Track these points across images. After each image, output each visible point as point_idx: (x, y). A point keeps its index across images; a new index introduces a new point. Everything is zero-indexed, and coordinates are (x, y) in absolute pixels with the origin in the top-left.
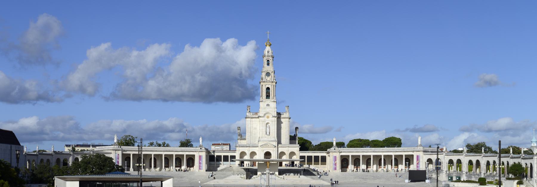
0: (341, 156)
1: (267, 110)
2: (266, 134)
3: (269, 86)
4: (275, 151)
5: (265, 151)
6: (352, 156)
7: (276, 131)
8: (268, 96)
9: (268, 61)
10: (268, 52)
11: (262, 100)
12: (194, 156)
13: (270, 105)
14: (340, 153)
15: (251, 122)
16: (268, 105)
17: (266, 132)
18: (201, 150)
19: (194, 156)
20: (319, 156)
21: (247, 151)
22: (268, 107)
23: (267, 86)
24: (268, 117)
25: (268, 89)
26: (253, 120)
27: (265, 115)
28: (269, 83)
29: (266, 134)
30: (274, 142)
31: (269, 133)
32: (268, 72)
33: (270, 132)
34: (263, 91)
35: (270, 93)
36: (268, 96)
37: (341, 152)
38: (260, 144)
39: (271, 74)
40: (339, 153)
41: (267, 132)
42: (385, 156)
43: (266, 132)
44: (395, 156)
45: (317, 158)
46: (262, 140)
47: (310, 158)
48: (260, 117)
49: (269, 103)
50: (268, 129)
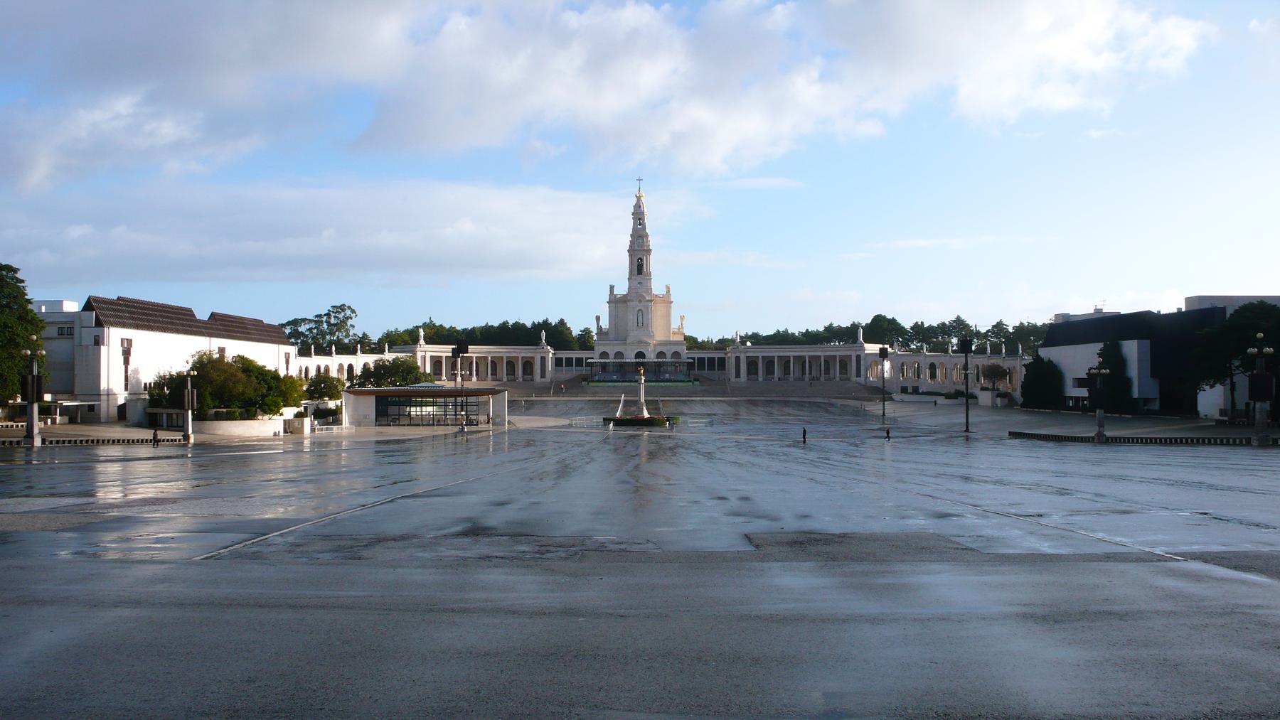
0: (747, 357)
5: (636, 352)
12: (533, 358)
19: (533, 358)
24: (640, 301)
37: (747, 352)
42: (809, 357)
44: (824, 356)
45: (711, 360)
47: (701, 360)
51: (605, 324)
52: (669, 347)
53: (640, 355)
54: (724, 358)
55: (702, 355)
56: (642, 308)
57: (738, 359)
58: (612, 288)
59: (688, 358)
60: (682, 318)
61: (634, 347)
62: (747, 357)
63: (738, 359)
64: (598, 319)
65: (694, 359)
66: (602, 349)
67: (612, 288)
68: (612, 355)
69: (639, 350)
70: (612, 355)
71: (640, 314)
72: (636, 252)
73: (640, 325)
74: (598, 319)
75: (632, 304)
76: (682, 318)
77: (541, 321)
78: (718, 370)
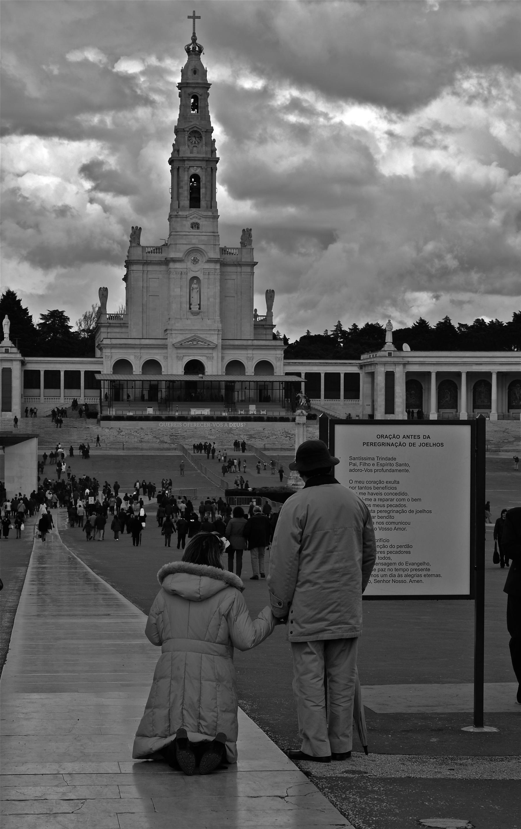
0: (408, 374)
1: (194, 241)
2: (190, 309)
3: (198, 171)
4: (215, 358)
5: (186, 360)
6: (469, 374)
7: (218, 300)
14: (405, 364)
15: (145, 276)
16: (195, 226)
17: (190, 304)
20: (339, 374)
23: (193, 171)
24: (195, 261)
26: (150, 268)
27: (189, 253)
28: (198, 163)
29: (190, 309)
30: (213, 332)
31: (198, 307)
32: (195, 129)
33: (199, 305)
34: (182, 184)
35: (202, 191)
37: (408, 363)
38: (175, 338)
39: (204, 138)
40: (401, 367)
41: (193, 304)
43: (190, 304)
46: (178, 325)
48: (174, 260)
49: (198, 221)
50: (195, 295)
54: (358, 374)
55: (315, 369)
56: (201, 277)
57: (390, 377)
59: (287, 374)
61: (184, 351)
62: (408, 374)
63: (390, 377)
65: (299, 374)
66: (119, 355)
68: (137, 369)
69: (192, 358)
70: (137, 369)
71: (194, 286)
72: (187, 164)
73: (195, 308)
75: (178, 265)
78: (345, 398)
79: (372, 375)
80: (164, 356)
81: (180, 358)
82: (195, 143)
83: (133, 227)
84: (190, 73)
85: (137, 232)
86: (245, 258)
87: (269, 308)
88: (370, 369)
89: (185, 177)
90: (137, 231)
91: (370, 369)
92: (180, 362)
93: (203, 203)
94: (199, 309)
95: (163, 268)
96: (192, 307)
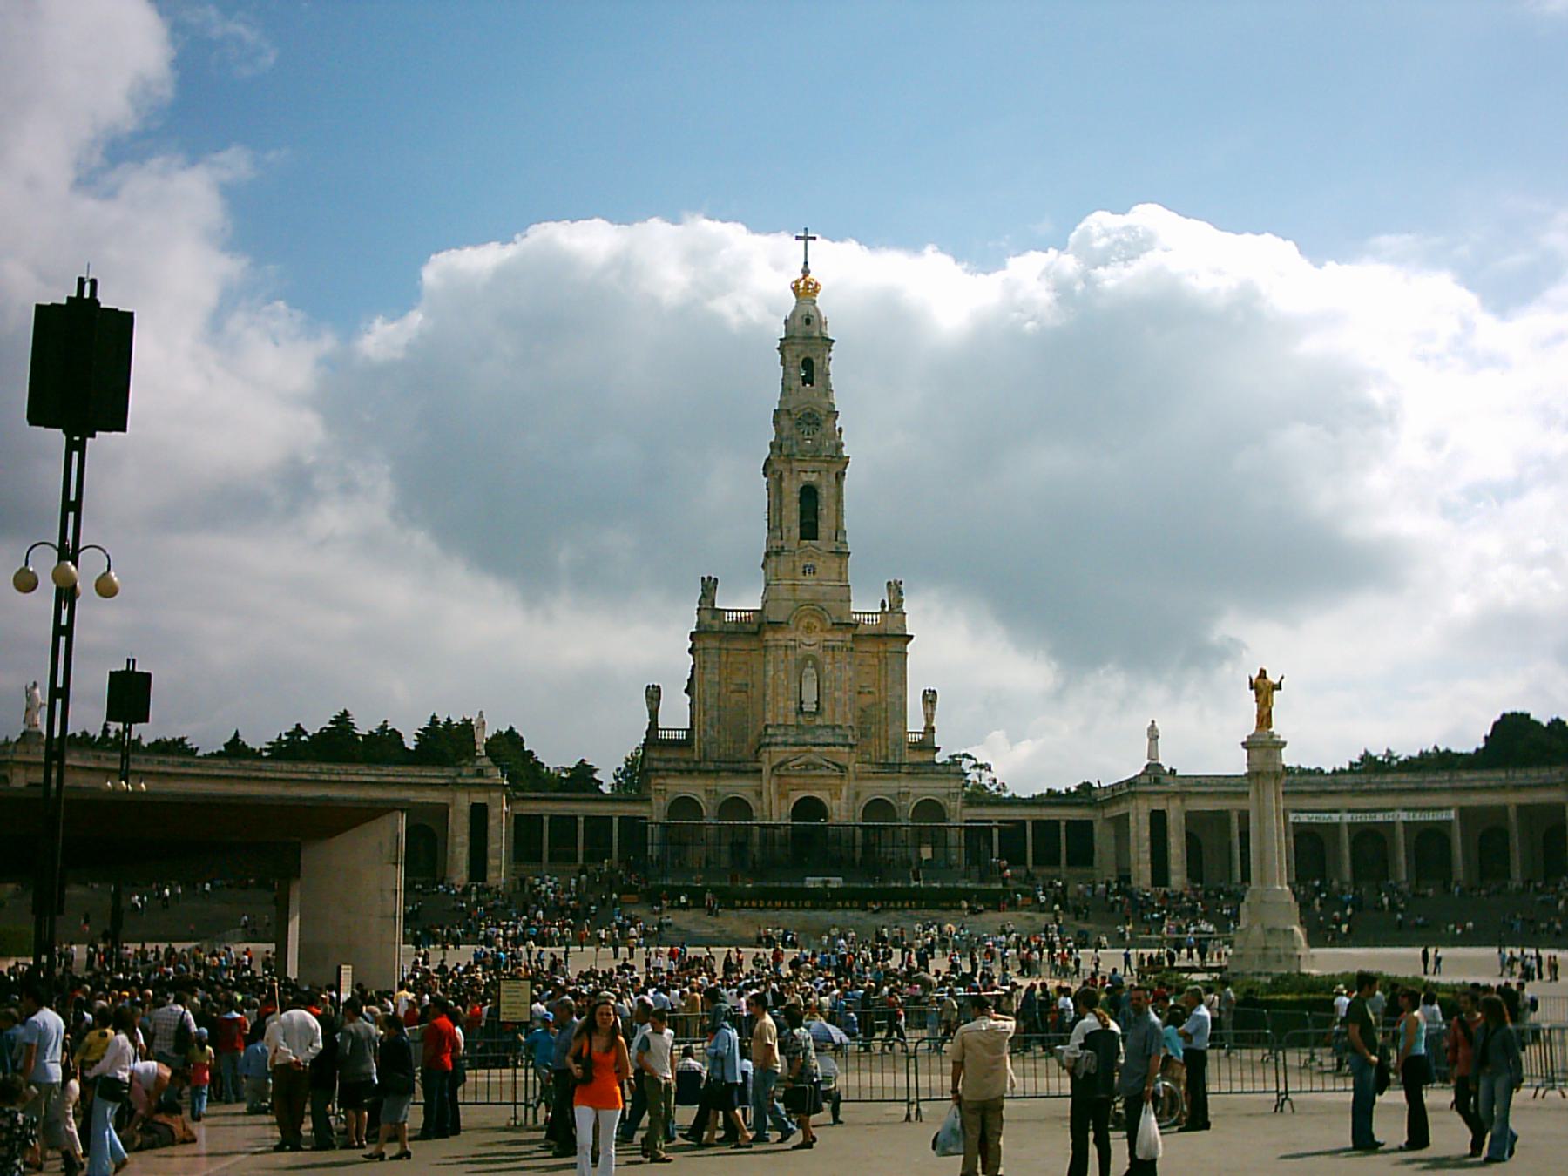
0: (1189, 816)
3: (813, 478)
8: (809, 530)
9: (808, 364)
10: (808, 321)
11: (780, 543)
13: (817, 570)
17: (801, 703)
18: (478, 781)
20: (1057, 823)
21: (702, 793)
22: (809, 579)
23: (805, 478)
25: (809, 495)
29: (801, 709)
31: (815, 706)
34: (786, 501)
36: (809, 530)
51: (676, 715)
52: (905, 783)
53: (809, 808)
58: (709, 587)
60: (930, 698)
62: (1189, 816)
64: (654, 695)
67: (709, 587)
69: (807, 794)
74: (654, 695)
76: (930, 698)
77: (456, 720)
79: (1121, 822)
80: (756, 792)
81: (784, 795)
82: (808, 434)
83: (703, 579)
84: (799, 322)
85: (711, 585)
86: (892, 628)
87: (929, 718)
88: (1115, 811)
89: (792, 488)
90: (711, 585)
91: (1115, 811)
92: (784, 802)
93: (824, 528)
94: (818, 709)
95: (754, 644)
96: (804, 706)
